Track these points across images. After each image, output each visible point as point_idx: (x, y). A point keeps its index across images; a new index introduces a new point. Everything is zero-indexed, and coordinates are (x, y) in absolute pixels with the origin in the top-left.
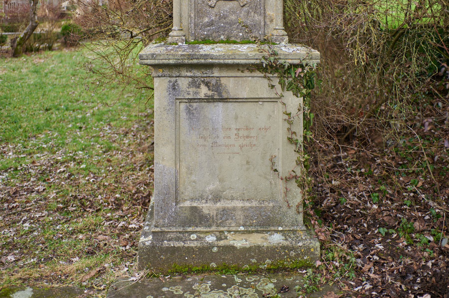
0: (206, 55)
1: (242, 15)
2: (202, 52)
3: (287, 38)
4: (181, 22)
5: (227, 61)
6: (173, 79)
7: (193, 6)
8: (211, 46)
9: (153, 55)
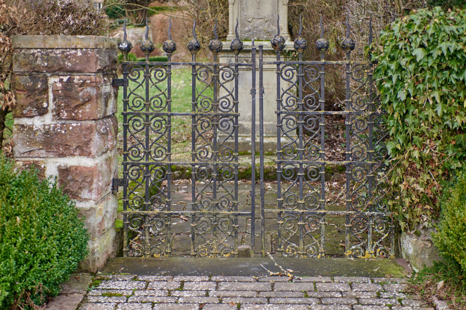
0: (246, 45)
1: (266, 26)
3: (289, 38)
6: (229, 58)
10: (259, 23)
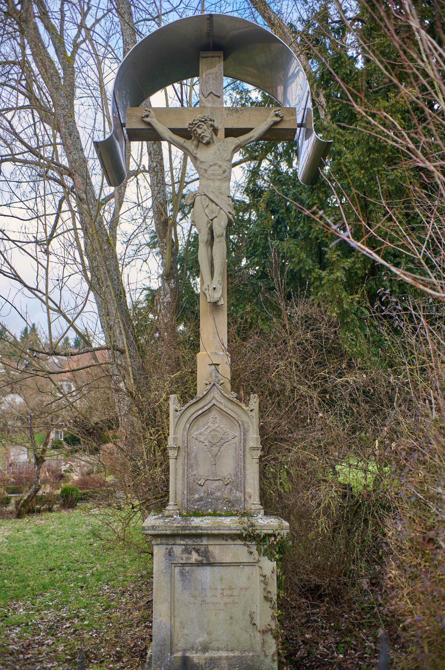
0: (196, 527)
1: (226, 492)
2: (193, 524)
3: (262, 512)
4: (176, 498)
5: (213, 532)
6: (169, 547)
7: (186, 484)
8: (200, 519)
9: (153, 526)
10: (216, 487)
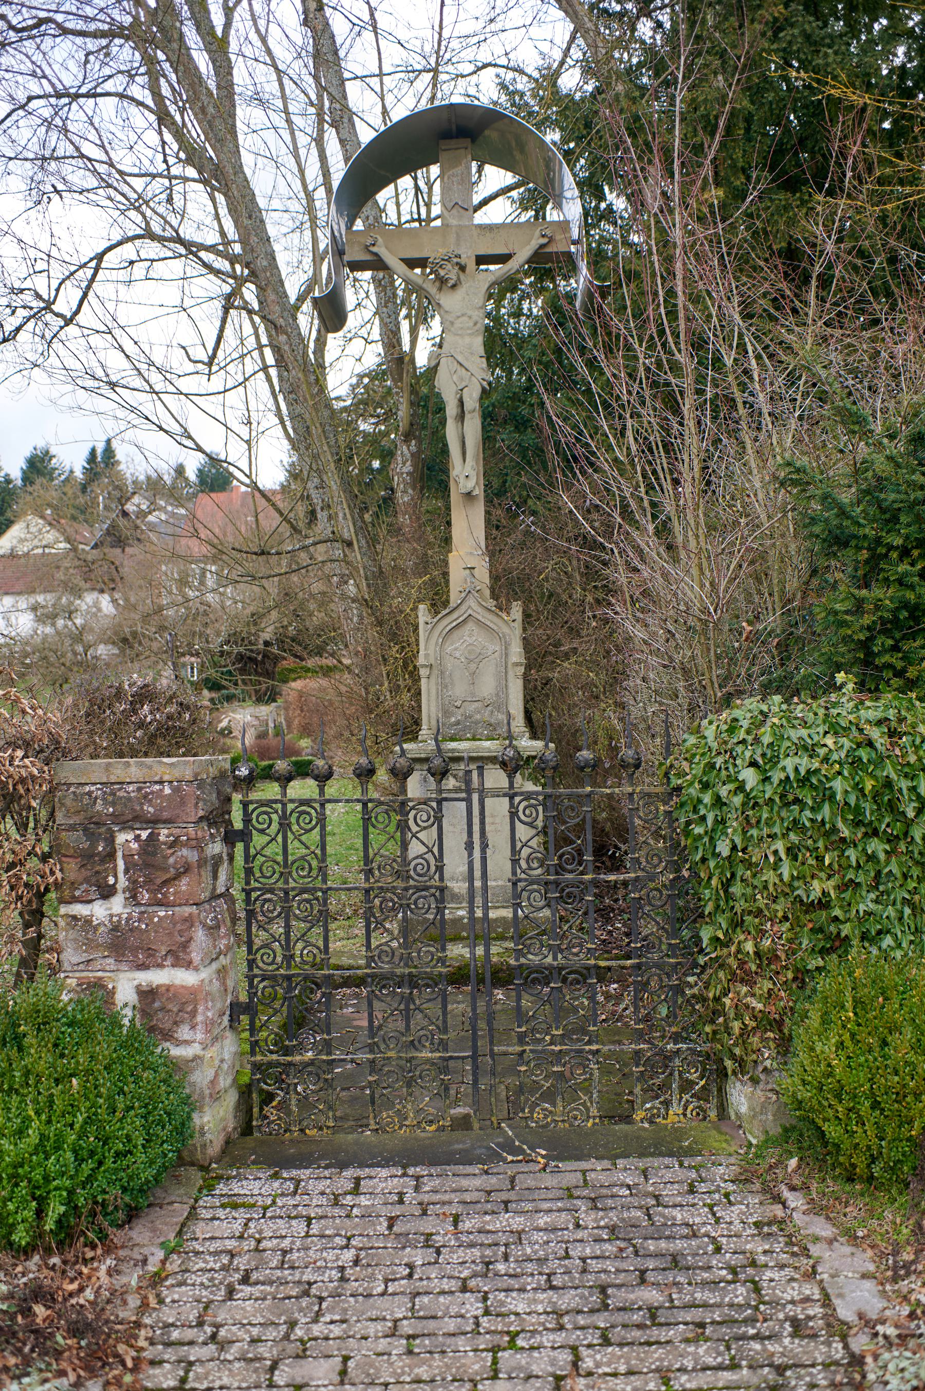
3: (527, 735)
